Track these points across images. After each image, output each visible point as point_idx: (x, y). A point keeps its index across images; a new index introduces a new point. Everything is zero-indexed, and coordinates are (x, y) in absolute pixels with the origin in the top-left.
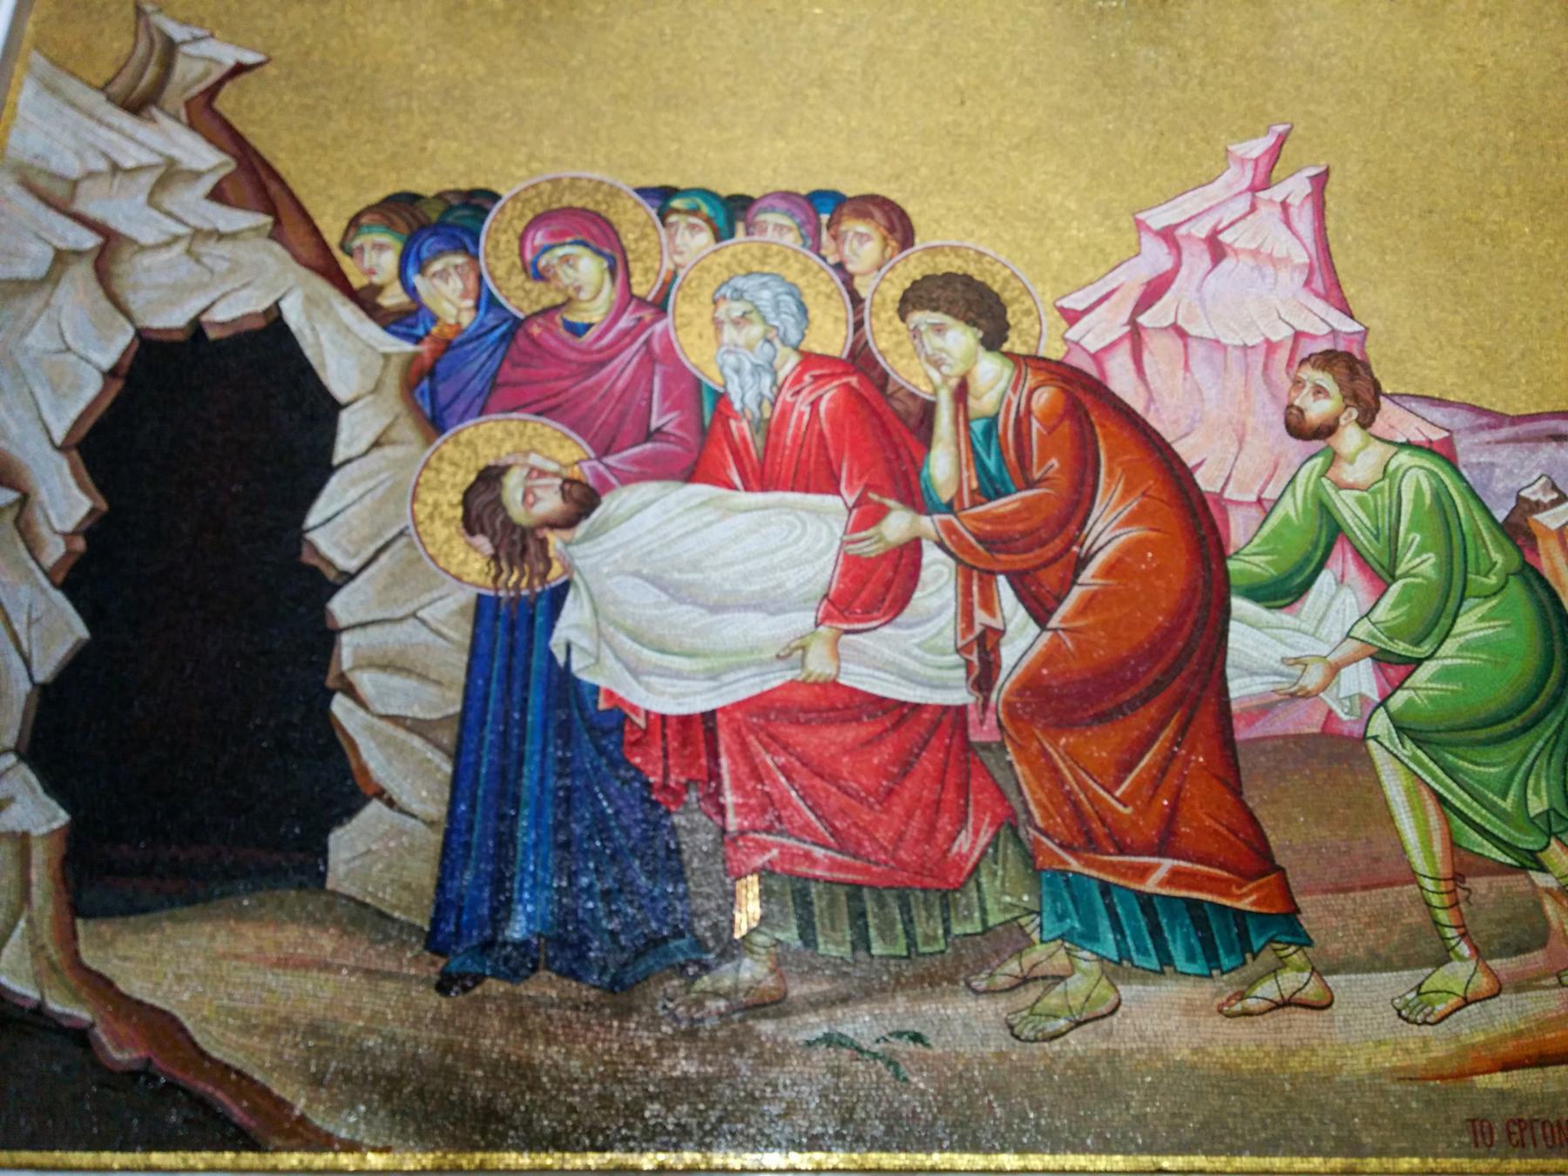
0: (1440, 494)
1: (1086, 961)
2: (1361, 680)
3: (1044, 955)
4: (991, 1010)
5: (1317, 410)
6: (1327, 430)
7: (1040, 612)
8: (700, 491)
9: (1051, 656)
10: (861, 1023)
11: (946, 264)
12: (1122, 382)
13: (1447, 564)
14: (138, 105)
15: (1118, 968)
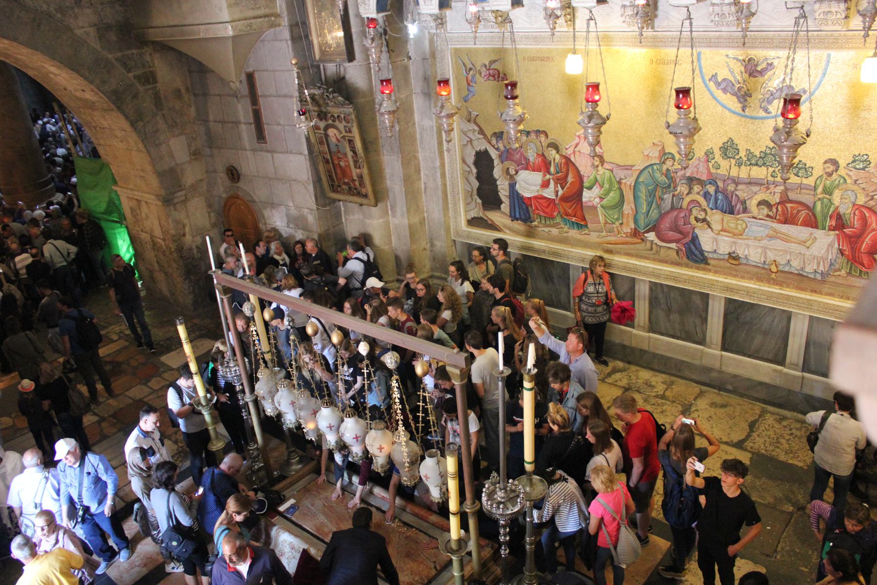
0: (610, 177)
1: (566, 227)
2: (597, 200)
3: (562, 225)
4: (557, 230)
5: (596, 163)
6: (598, 166)
7: (563, 189)
8: (527, 171)
9: (564, 194)
10: (546, 229)
11: (553, 141)
12: (572, 159)
13: (610, 186)
14: (469, 121)
15: (569, 228)
